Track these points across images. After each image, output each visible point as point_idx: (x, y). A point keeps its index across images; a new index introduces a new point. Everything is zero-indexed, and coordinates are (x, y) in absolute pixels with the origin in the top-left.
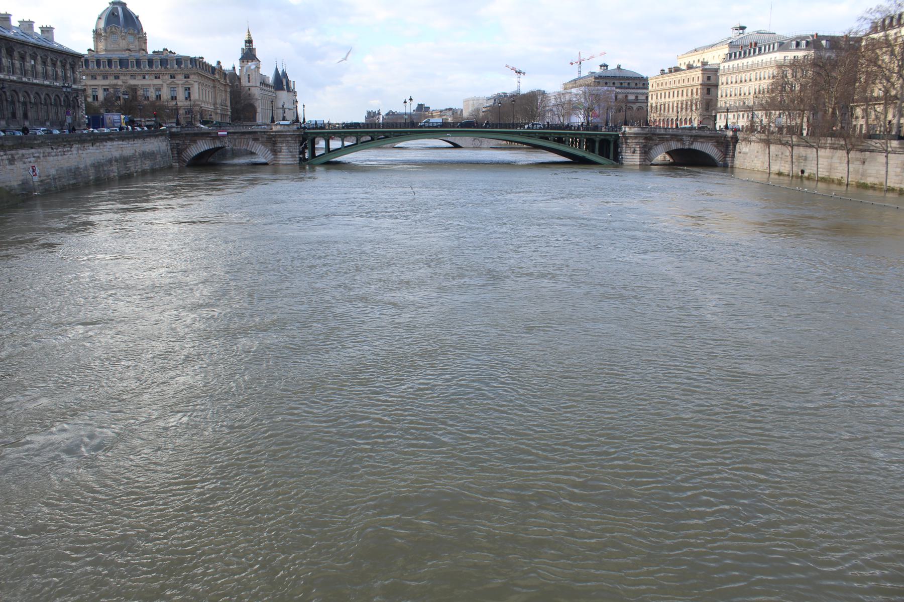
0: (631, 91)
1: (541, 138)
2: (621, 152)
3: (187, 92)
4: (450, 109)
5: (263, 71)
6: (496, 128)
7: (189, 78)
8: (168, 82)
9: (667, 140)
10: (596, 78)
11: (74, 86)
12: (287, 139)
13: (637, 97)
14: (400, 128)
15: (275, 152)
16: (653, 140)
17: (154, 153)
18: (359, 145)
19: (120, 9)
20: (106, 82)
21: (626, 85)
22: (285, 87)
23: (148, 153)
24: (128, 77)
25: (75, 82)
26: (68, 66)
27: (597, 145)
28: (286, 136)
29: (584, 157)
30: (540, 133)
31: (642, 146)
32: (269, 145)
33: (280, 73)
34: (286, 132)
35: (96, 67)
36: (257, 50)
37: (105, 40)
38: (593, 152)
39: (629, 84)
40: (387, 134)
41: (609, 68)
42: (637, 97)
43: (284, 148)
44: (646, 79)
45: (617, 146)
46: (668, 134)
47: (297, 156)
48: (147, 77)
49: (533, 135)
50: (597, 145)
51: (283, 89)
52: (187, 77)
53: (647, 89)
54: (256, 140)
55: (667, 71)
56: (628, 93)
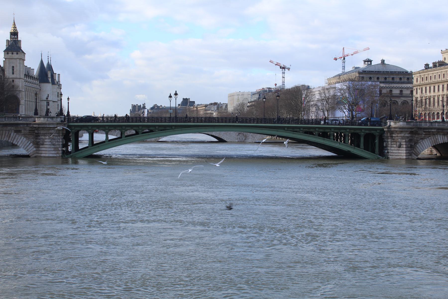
0: (395, 85)
1: (306, 133)
2: (387, 147)
4: (215, 104)
5: (26, 63)
6: (261, 123)
9: (434, 134)
10: (359, 73)
12: (51, 131)
13: (401, 91)
14: (165, 122)
15: (37, 145)
16: (419, 134)
18: (123, 138)
21: (390, 80)
22: (50, 80)
27: (362, 140)
29: (349, 151)
30: (304, 128)
31: (407, 140)
33: (45, 65)
34: (49, 124)
36: (22, 42)
38: (358, 146)
39: (393, 78)
40: (152, 128)
41: (373, 63)
42: (401, 91)
43: (47, 141)
44: (411, 74)
45: (382, 140)
46: (435, 128)
47: (60, 149)
49: (298, 130)
50: (362, 140)
51: (47, 82)
53: (412, 83)
54: (18, 132)
55: (431, 65)
56: (393, 88)
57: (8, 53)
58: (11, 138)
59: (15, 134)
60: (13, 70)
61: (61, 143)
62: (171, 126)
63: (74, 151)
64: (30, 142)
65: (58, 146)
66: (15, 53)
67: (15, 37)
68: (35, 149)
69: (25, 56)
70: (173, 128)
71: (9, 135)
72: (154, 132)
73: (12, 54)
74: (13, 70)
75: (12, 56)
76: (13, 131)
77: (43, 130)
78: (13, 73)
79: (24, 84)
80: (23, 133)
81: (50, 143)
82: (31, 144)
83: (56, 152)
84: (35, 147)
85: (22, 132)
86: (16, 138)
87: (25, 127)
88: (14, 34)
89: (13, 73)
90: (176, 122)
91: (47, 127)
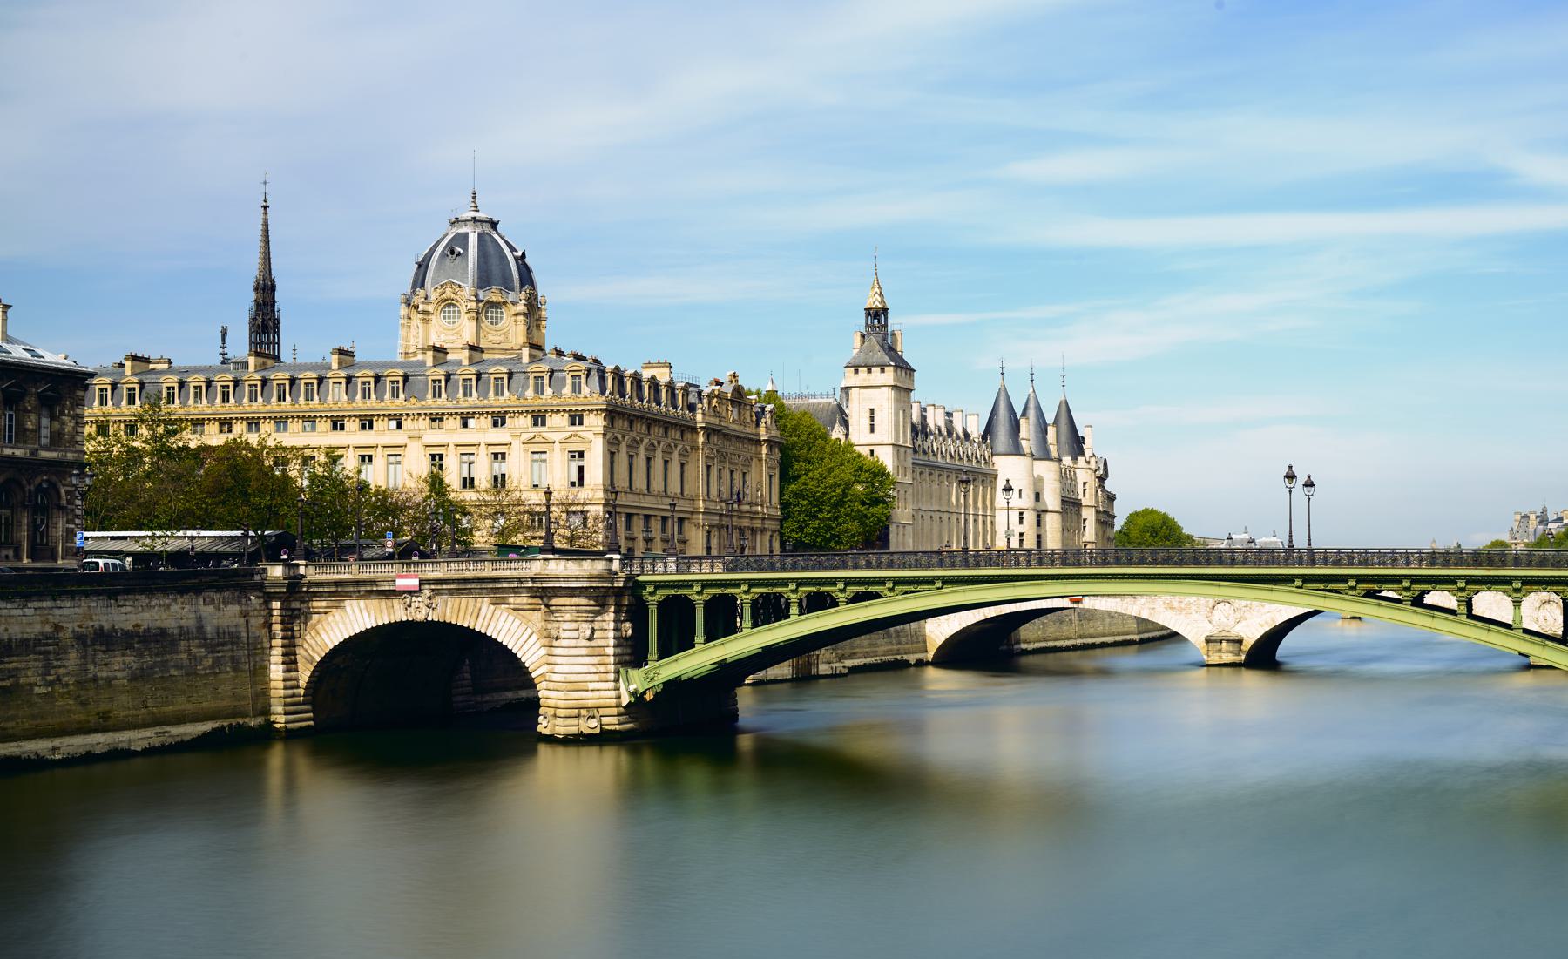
3: (574, 465)
7: (581, 423)
8: (525, 437)
11: (44, 454)
15: (551, 639)
17: (163, 632)
19: (473, 240)
20: (434, 436)
23: (128, 635)
24: (424, 423)
25: (56, 440)
26: (30, 403)
28: (571, 592)
32: (537, 617)
34: (566, 579)
35: (346, 397)
37: (426, 321)
48: (471, 422)
52: (576, 418)
57: (856, 372)
58: (480, 619)
59: (492, 607)
60: (872, 419)
61: (611, 634)
62: (930, 581)
63: (656, 658)
64: (529, 631)
65: (601, 643)
66: (876, 370)
67: (879, 322)
68: (543, 651)
69: (911, 376)
70: (939, 584)
71: (476, 611)
72: (882, 597)
73: (869, 371)
74: (872, 419)
75: (869, 380)
76: (486, 599)
77: (556, 596)
78: (872, 430)
79: (910, 460)
80: (512, 606)
81: (575, 634)
82: (534, 637)
83: (595, 660)
84: (544, 646)
85: (508, 604)
86: (494, 619)
87: (516, 590)
88: (877, 315)
89: (872, 430)
90: (967, 566)
91: (561, 587)
